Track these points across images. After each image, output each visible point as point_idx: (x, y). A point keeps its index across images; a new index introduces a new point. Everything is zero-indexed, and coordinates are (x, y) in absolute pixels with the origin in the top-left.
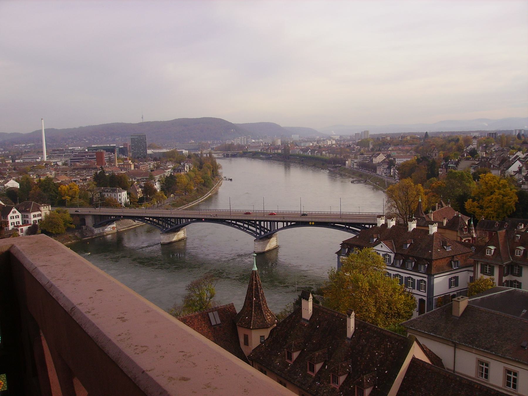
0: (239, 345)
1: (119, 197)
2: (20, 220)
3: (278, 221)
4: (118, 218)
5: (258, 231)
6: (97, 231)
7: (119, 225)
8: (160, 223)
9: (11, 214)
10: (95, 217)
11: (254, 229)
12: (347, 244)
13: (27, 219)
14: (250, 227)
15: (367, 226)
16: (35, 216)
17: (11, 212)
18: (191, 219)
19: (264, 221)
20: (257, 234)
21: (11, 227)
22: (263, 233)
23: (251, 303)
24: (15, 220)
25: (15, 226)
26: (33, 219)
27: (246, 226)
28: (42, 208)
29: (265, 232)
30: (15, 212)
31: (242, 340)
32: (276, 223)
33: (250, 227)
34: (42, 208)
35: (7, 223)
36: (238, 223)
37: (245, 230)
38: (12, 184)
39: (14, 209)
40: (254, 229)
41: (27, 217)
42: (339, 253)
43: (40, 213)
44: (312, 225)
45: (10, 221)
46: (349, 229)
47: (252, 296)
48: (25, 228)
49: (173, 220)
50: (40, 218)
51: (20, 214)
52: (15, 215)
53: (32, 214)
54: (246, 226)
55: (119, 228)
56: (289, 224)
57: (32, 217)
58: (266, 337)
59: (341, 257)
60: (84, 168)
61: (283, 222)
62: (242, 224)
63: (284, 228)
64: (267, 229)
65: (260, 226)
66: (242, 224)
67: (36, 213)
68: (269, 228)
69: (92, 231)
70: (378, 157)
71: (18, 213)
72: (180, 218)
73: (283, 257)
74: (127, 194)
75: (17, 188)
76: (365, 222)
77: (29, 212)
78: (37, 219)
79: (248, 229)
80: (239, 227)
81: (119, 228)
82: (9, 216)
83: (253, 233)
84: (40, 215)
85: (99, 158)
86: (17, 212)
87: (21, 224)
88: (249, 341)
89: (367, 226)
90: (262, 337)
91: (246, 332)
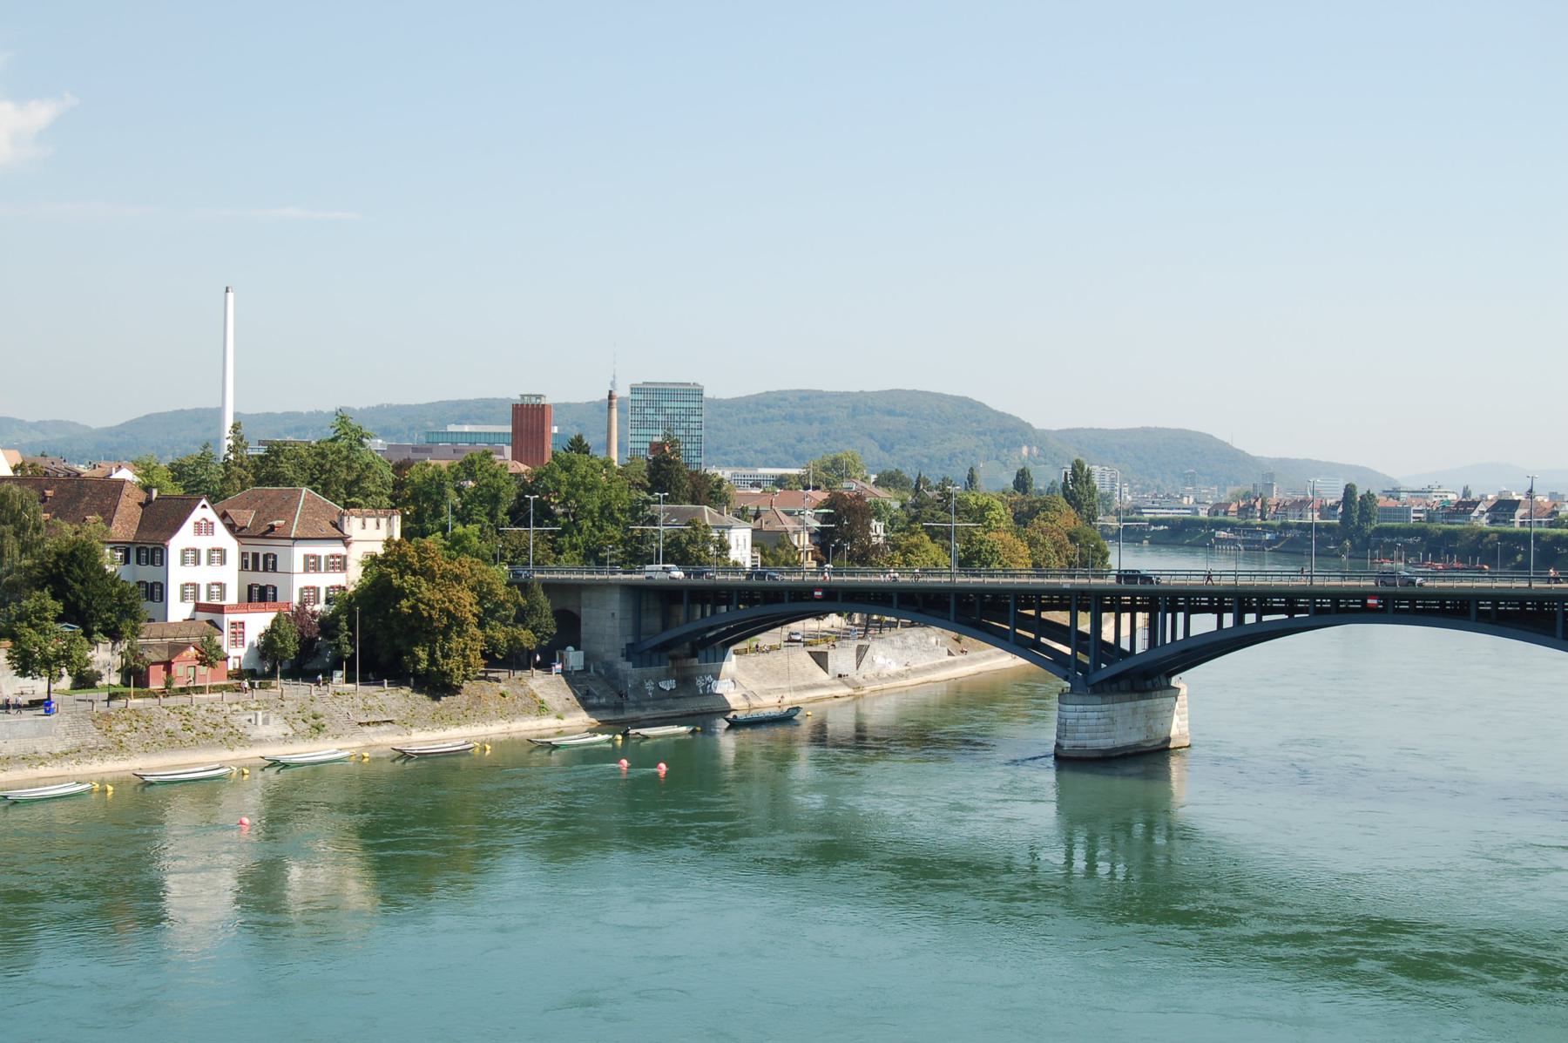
2: (230, 576)
16: (312, 564)
17: (188, 526)
21: (178, 610)
24: (203, 575)
25: (199, 607)
26: (301, 580)
28: (353, 526)
34: (353, 526)
35: (156, 591)
41: (270, 564)
43: (339, 549)
45: (177, 575)
48: (258, 623)
50: (337, 579)
51: (232, 546)
52: (204, 543)
53: (300, 552)
57: (298, 564)
67: (323, 550)
71: (222, 537)
78: (325, 581)
84: (340, 564)
86: (220, 527)
87: (232, 598)
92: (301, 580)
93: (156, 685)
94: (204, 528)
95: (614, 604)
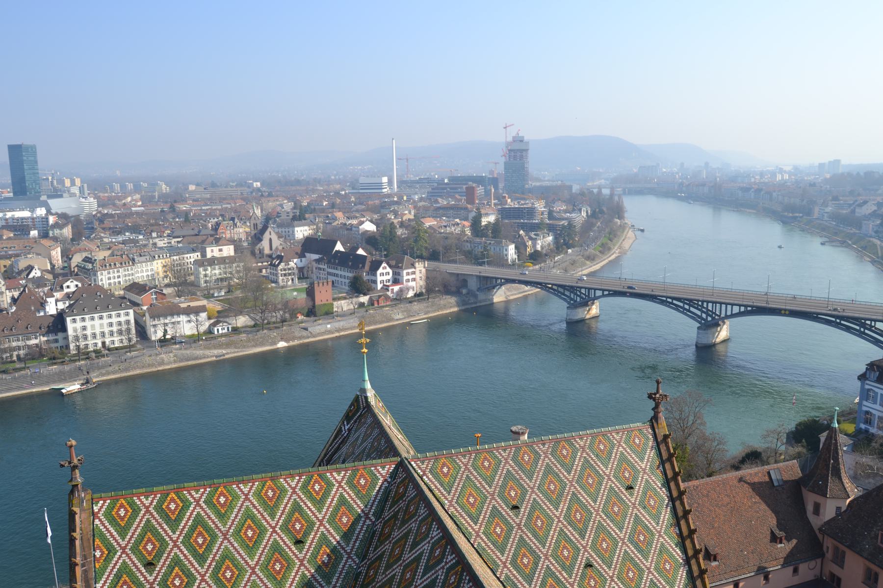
0: (805, 512)
1: (505, 252)
2: (390, 277)
3: (732, 305)
4: (509, 281)
5: (704, 316)
6: (481, 296)
7: (508, 289)
8: (567, 293)
9: (380, 271)
10: (479, 278)
11: (699, 313)
12: (878, 367)
13: (397, 277)
14: (692, 309)
15: (868, 322)
16: (408, 274)
17: (381, 268)
18: (609, 291)
19: (713, 302)
20: (703, 319)
21: (380, 286)
22: (709, 319)
23: (828, 466)
24: (385, 278)
27: (687, 307)
28: (417, 265)
29: (713, 318)
30: (385, 268)
31: (810, 508)
32: (729, 307)
33: (692, 309)
35: (375, 282)
36: (674, 302)
37: (684, 311)
38: (369, 227)
39: (384, 265)
40: (699, 313)
41: (399, 274)
42: (862, 377)
44: (785, 315)
45: (379, 278)
46: (840, 323)
47: (829, 457)
49: (583, 291)
50: (414, 276)
52: (385, 271)
53: (405, 272)
54: (687, 307)
55: (509, 293)
56: (749, 309)
58: (843, 509)
59: (868, 382)
60: (452, 208)
61: (740, 306)
62: (681, 304)
63: (740, 314)
64: (715, 313)
65: (705, 310)
66: (681, 304)
67: (410, 271)
68: (718, 313)
69: (476, 296)
70: (865, 207)
71: (389, 270)
72: (595, 289)
73: (734, 352)
74: (516, 248)
75: (373, 232)
76: (867, 316)
77: (401, 268)
79: (689, 311)
80: (677, 308)
81: (509, 293)
82: (379, 272)
83: (694, 317)
84: (414, 273)
85: (470, 194)
88: (822, 511)
89: (868, 322)
90: (838, 508)
91: (819, 499)
92: (405, 278)
93: (376, 305)
94: (384, 268)
95: (475, 279)
